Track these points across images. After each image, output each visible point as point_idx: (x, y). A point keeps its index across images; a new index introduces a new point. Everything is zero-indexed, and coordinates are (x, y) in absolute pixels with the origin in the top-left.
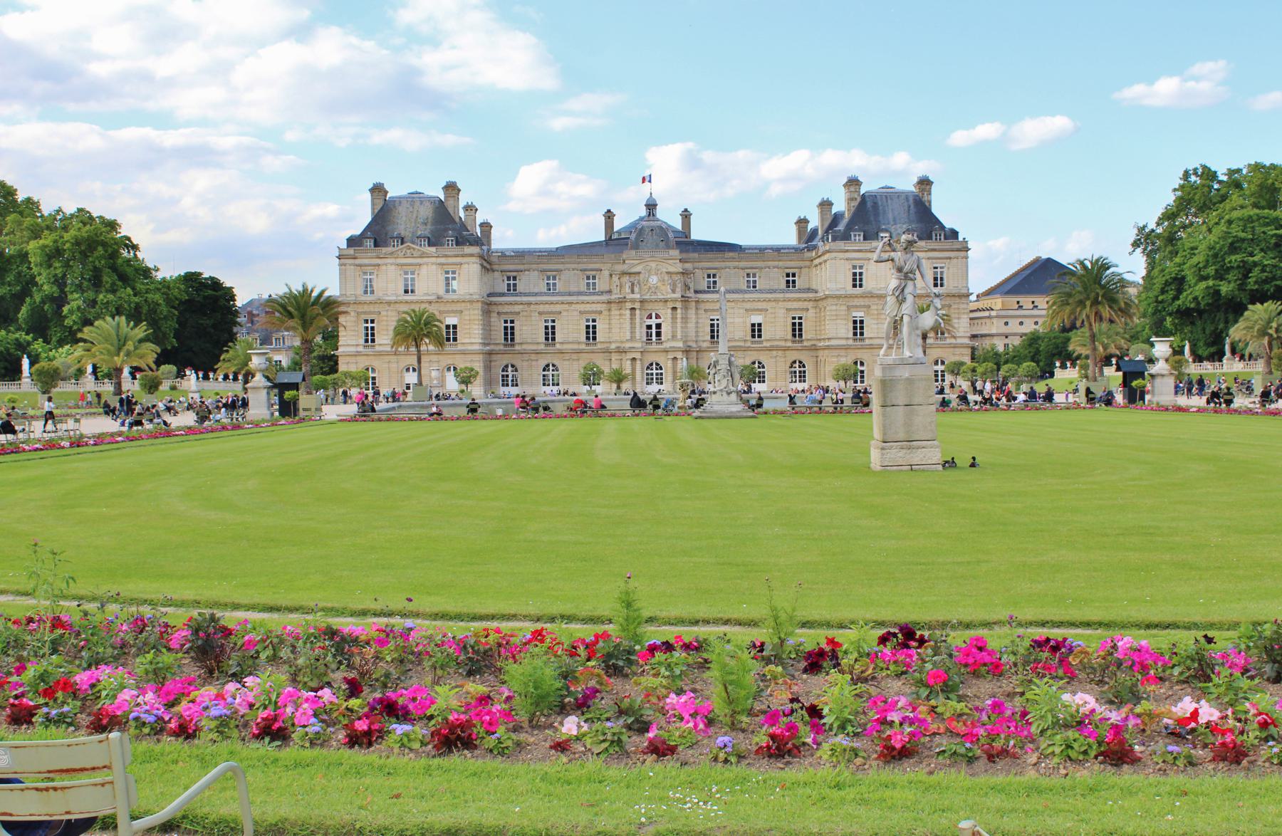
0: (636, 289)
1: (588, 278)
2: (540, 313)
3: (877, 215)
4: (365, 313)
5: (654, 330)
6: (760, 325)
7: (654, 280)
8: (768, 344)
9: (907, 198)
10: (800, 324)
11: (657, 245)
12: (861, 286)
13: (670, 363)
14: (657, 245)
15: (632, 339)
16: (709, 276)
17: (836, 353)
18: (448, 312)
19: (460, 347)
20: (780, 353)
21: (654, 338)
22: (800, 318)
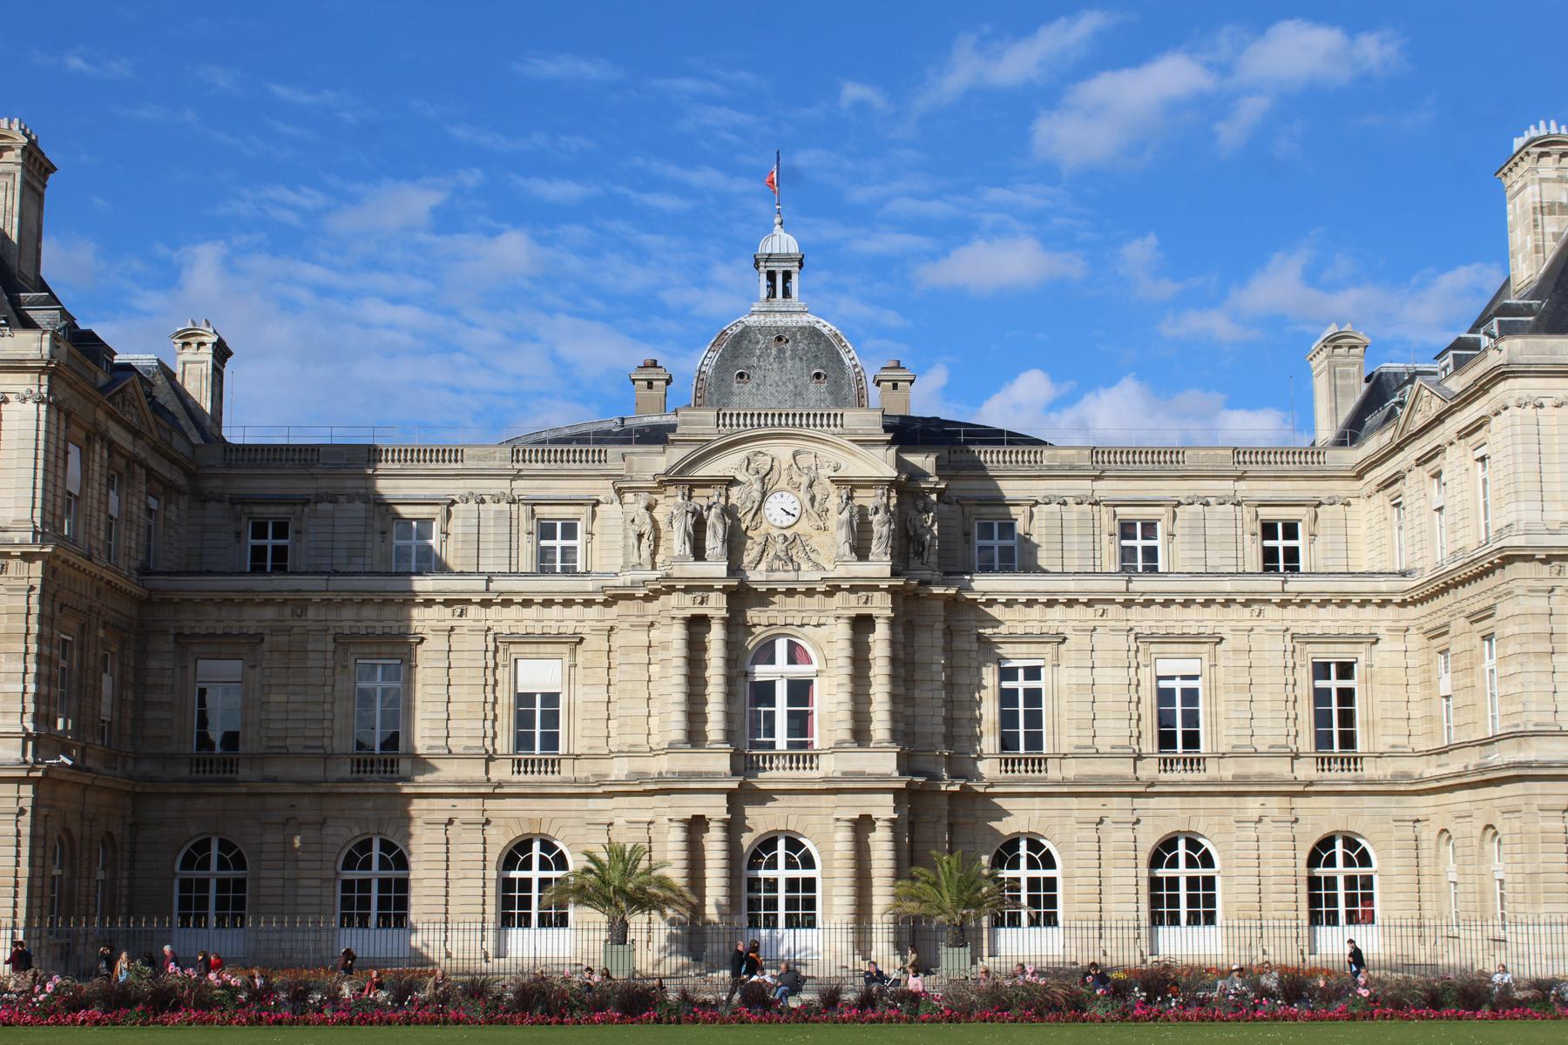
0: (714, 542)
1: (547, 531)
2: (343, 641)
5: (781, 708)
6: (1191, 696)
7: (780, 510)
8: (1228, 770)
10: (1346, 696)
11: (798, 394)
13: (842, 841)
14: (798, 394)
15: (695, 736)
16: (986, 531)
21: (781, 739)
22: (1346, 670)
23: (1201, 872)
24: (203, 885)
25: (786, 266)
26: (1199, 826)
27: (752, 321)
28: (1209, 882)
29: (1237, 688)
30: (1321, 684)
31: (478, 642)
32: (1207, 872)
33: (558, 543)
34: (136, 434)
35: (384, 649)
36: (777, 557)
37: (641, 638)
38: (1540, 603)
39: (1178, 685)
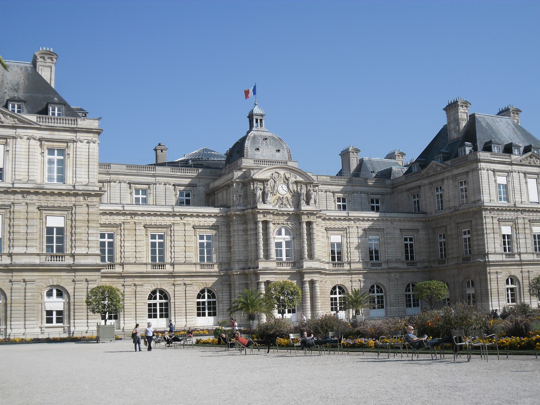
5: (284, 249)
7: (282, 190)
17: (493, 269)
18: (53, 208)
20: (398, 275)
22: (411, 239)
30: (406, 242)
31: (189, 228)
35: (159, 229)
36: (282, 204)
37: (241, 227)
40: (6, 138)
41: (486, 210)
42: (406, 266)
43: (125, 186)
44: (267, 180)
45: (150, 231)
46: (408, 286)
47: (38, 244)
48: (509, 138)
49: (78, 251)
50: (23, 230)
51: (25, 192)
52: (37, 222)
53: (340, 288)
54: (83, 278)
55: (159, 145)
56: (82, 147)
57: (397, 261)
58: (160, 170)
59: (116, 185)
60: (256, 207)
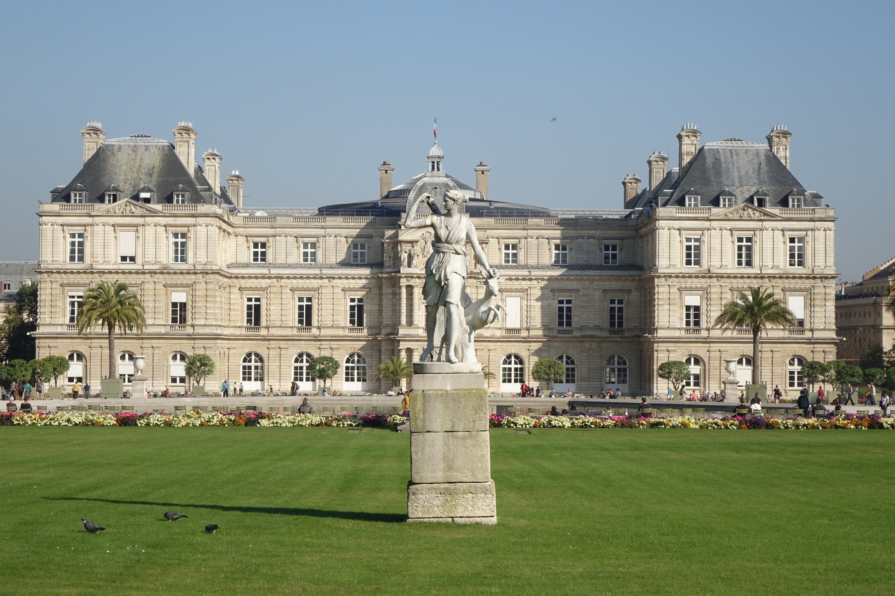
3: (718, 174)
4: (69, 285)
9: (757, 153)
10: (620, 310)
12: (697, 263)
18: (177, 286)
19: (189, 330)
20: (594, 345)
22: (620, 302)
23: (571, 366)
24: (250, 368)
25: (438, 160)
26: (571, 353)
27: (426, 179)
28: (573, 370)
29: (584, 307)
30: (612, 306)
31: (338, 291)
32: (573, 366)
33: (359, 251)
34: (224, 221)
37: (390, 291)
38: (661, 289)
39: (565, 305)
40: (136, 226)
41: (659, 277)
42: (607, 334)
43: (291, 240)
44: (417, 242)
45: (297, 294)
46: (613, 357)
47: (164, 316)
48: (740, 178)
49: (197, 322)
50: (151, 304)
51: (153, 273)
52: (163, 298)
53: (516, 357)
54: (202, 346)
55: (384, 164)
56: (202, 230)
57: (596, 328)
58: (331, 221)
59: (283, 238)
60: (399, 272)
